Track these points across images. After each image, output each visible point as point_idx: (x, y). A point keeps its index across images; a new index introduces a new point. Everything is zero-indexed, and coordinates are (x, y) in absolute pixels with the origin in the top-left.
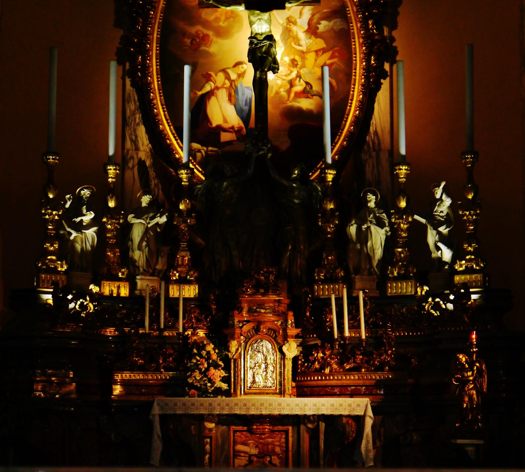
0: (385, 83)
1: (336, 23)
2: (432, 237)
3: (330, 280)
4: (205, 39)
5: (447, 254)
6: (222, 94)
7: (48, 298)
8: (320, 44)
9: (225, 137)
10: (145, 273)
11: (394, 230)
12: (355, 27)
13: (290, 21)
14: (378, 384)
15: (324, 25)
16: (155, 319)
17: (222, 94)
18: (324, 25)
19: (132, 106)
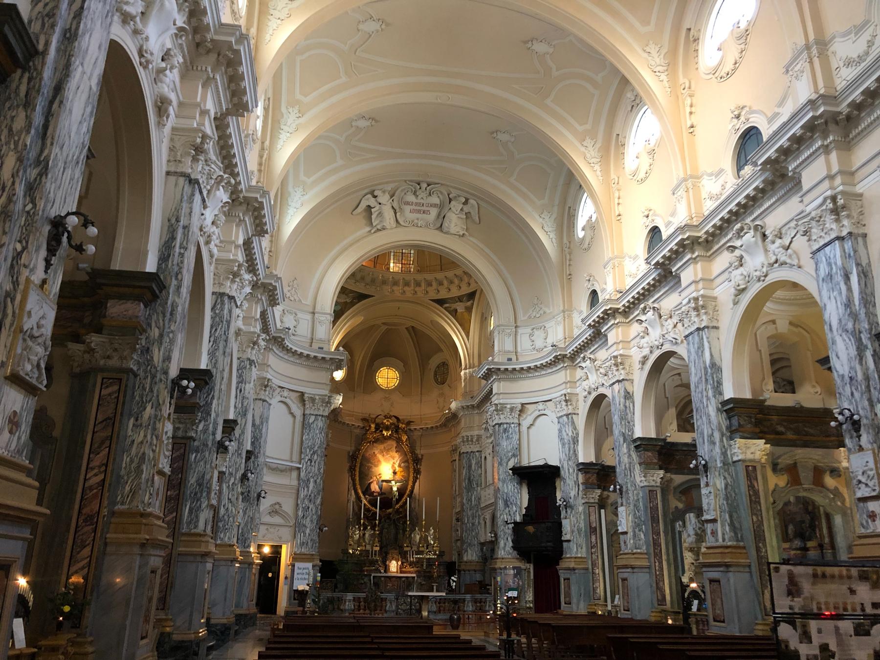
0: (418, 481)
1: (406, 464)
2: (429, 538)
3: (407, 546)
4: (371, 467)
5: (432, 542)
6: (375, 482)
7: (351, 551)
8: (402, 469)
9: (375, 494)
10: (369, 544)
11: (422, 536)
12: (411, 465)
13: (394, 463)
14: (417, 571)
15: (402, 465)
16: (372, 556)
17: (375, 482)
18: (402, 465)
19: (351, 485)
